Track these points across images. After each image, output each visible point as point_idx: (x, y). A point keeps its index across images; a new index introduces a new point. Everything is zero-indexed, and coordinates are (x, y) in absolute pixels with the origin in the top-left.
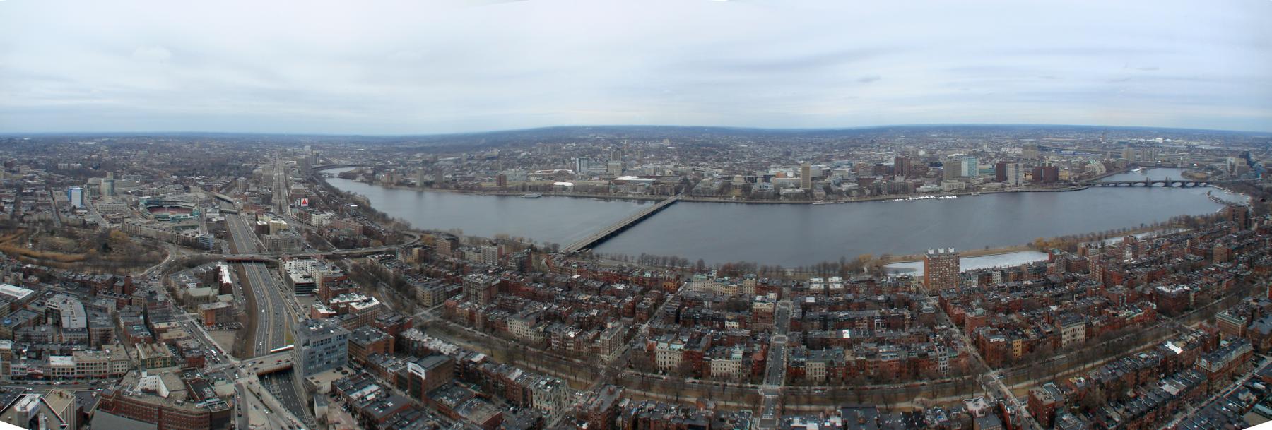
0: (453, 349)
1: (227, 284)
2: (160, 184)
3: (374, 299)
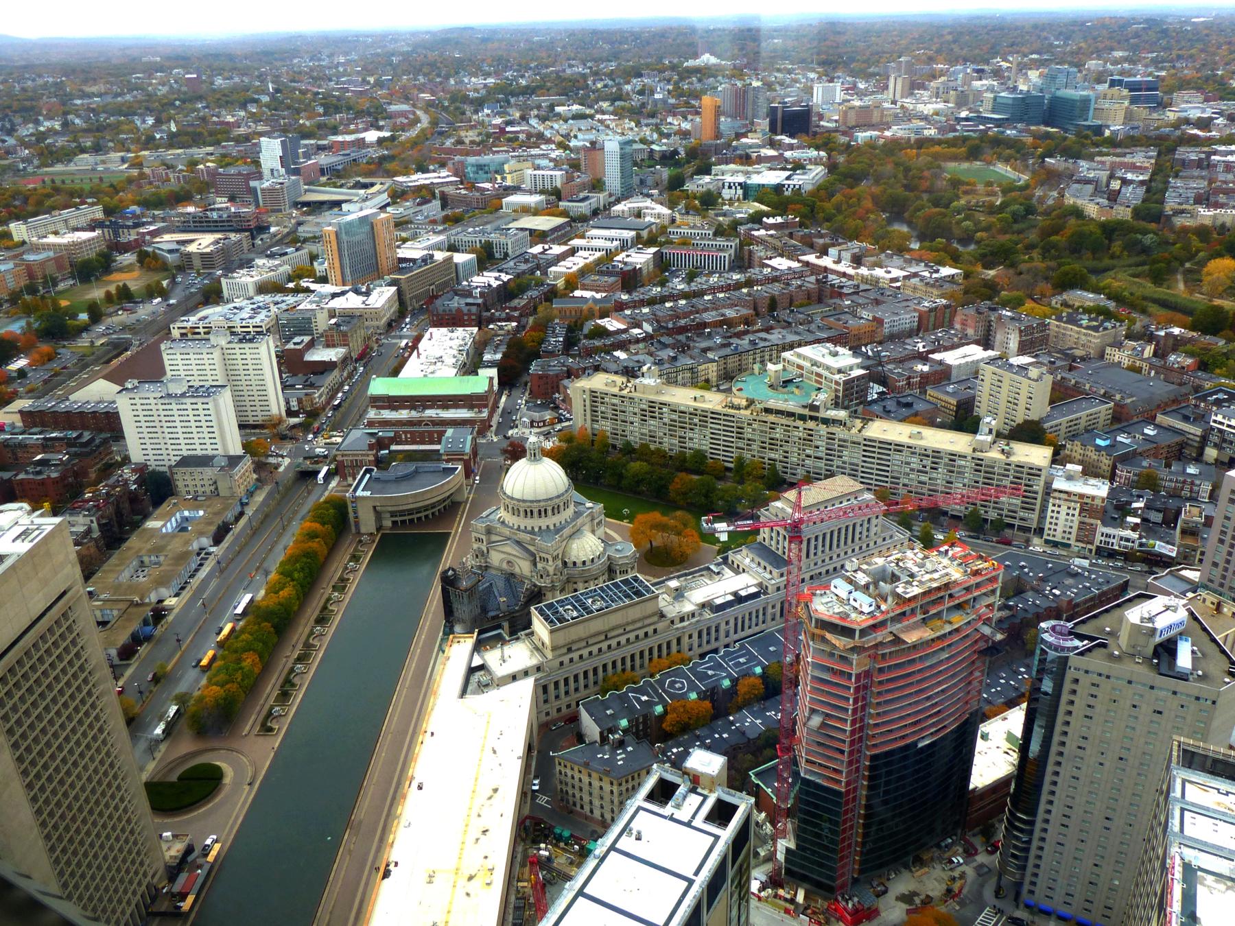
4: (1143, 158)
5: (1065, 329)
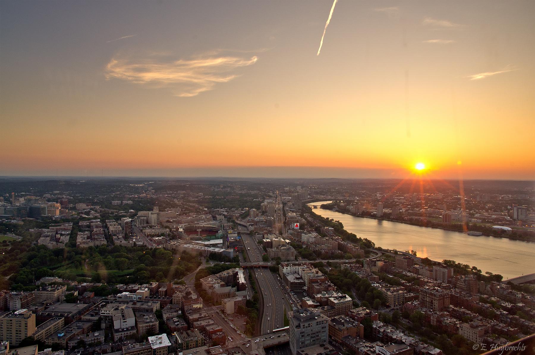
0: (413, 341)
1: (243, 283)
2: (194, 214)
3: (347, 296)
4: (69, 226)
5: (41, 293)
